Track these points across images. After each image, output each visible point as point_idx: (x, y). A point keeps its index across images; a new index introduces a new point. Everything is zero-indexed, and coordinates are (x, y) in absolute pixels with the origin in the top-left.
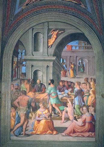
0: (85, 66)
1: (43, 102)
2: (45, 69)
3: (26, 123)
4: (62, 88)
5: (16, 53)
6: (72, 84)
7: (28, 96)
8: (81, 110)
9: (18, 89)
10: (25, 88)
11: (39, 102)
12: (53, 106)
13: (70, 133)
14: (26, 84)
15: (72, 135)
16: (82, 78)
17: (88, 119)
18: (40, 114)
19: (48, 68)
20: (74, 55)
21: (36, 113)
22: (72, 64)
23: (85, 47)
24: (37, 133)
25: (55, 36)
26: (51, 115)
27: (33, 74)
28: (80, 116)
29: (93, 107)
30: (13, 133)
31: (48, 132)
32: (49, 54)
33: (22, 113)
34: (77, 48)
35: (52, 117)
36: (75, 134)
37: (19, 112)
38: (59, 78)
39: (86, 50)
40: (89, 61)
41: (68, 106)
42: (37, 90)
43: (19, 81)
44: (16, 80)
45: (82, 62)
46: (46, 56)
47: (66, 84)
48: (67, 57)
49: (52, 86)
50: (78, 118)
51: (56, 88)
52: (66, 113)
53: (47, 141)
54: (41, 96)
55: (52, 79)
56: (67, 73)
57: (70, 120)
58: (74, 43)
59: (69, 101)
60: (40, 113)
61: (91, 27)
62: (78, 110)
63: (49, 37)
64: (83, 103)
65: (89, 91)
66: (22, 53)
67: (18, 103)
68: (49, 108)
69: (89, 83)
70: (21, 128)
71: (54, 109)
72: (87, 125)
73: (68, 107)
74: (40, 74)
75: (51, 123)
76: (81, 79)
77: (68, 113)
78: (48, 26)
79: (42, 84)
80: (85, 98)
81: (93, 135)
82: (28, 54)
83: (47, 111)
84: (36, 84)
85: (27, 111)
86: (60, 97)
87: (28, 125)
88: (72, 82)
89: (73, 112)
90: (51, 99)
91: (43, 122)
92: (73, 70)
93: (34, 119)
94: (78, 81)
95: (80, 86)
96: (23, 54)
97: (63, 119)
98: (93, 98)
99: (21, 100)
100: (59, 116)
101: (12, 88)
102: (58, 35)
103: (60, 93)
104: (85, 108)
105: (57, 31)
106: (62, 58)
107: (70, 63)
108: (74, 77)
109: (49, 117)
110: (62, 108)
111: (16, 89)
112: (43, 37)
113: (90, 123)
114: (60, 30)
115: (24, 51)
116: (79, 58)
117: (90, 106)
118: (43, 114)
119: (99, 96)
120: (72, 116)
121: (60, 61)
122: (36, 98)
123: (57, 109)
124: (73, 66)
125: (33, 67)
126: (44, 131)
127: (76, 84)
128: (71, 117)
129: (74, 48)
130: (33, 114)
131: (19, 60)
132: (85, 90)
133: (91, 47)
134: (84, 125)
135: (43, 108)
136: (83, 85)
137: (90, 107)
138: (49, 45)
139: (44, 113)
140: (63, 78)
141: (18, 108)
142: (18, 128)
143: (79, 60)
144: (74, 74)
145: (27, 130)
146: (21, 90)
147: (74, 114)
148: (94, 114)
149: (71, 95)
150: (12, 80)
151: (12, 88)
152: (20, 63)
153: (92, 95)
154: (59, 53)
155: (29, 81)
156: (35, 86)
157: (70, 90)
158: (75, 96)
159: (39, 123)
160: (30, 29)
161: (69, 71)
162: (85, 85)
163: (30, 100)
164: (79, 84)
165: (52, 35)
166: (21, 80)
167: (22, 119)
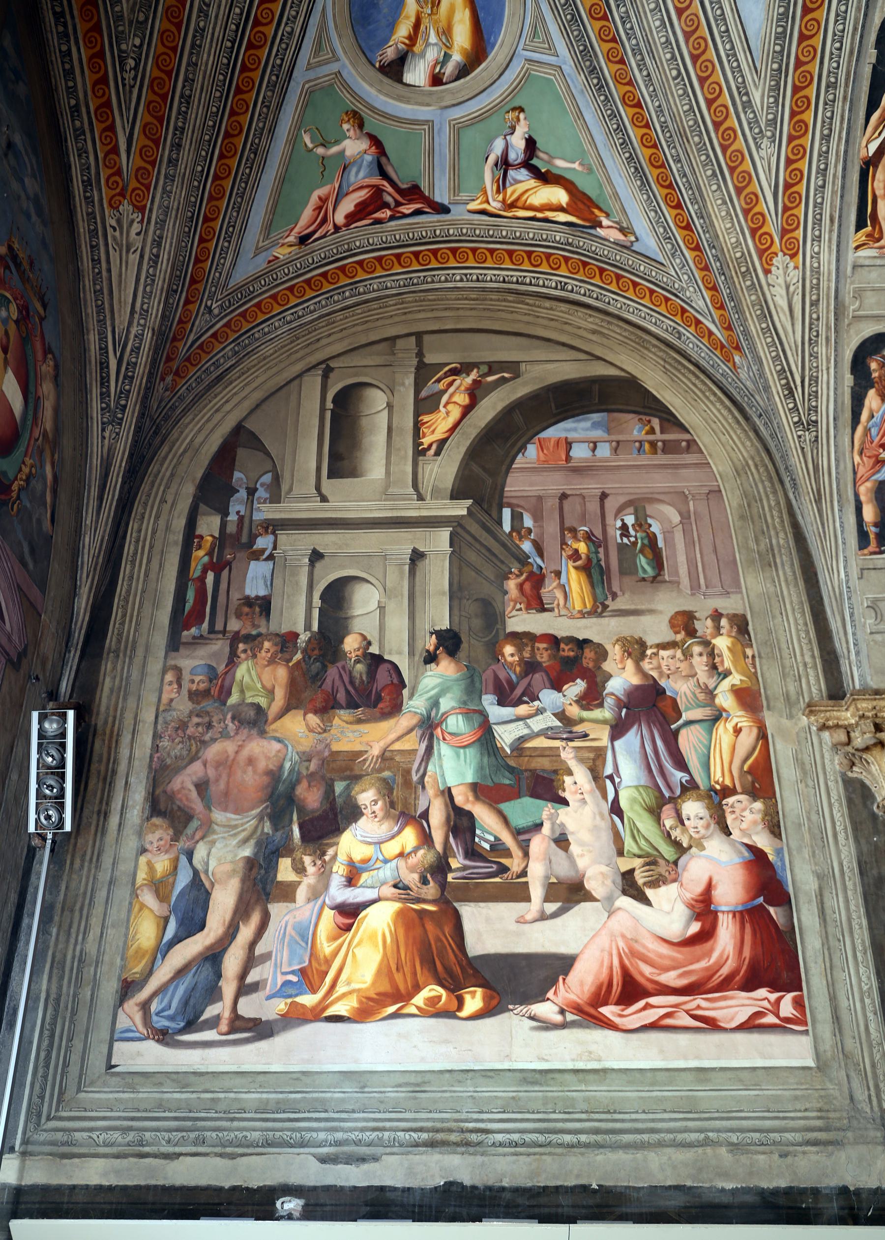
0: (661, 544)
1: (386, 774)
2: (402, 572)
3: (246, 933)
4: (522, 677)
5: (214, 489)
6: (589, 654)
7: (279, 741)
8: (668, 823)
9: (216, 688)
10: (259, 686)
11: (355, 778)
12: (459, 800)
13: (601, 997)
14: (272, 661)
15: (617, 1020)
16: (651, 612)
17: (730, 893)
18: (357, 857)
19: (420, 565)
20: (591, 486)
21: (331, 852)
22: (576, 538)
23: (653, 444)
24: (329, 1012)
25: (462, 399)
26: (440, 868)
27: (317, 602)
28: (662, 869)
29: (754, 794)
30: (138, 1017)
31: (419, 999)
32: (426, 488)
33: (223, 856)
34: (604, 451)
35: (450, 877)
36: (641, 1004)
37: (200, 853)
38: (492, 617)
39: (662, 459)
40: (685, 516)
41: (567, 795)
42: (341, 696)
43: (220, 646)
44: (199, 640)
45: (641, 524)
46: (404, 497)
47: (544, 657)
48: (540, 498)
49: (446, 669)
50: (655, 883)
51: (472, 689)
52: (553, 845)
53: (412, 1079)
54: (370, 738)
55: (445, 624)
56: (550, 589)
57: (588, 897)
58: (581, 433)
59: (573, 764)
60: (359, 852)
61: (677, 342)
62: (646, 825)
63: (426, 405)
64: (679, 776)
65: (711, 694)
66: (251, 492)
67: (202, 787)
68: (425, 815)
69: (706, 643)
70: (207, 971)
71: (461, 824)
72: (727, 934)
73: (565, 802)
74: (365, 602)
75: (439, 926)
76: (645, 620)
77: (574, 848)
78: (420, 355)
79: (376, 661)
80: (689, 741)
81: (787, 1008)
82: (295, 491)
83: (409, 837)
84: (333, 662)
85: (259, 844)
86: (506, 736)
87: (259, 950)
88: (586, 641)
89: (606, 837)
90: (444, 750)
91: (380, 919)
92: (587, 569)
93: (315, 894)
94: (626, 633)
95: (646, 665)
96: (261, 493)
97: (537, 892)
98: (748, 738)
99: (225, 764)
100: (504, 869)
101: (166, 688)
102: (475, 394)
103: (507, 712)
104: (693, 808)
105: (474, 375)
106: (509, 505)
107: (563, 529)
108: (599, 609)
109: (424, 881)
110: (522, 810)
111: (194, 696)
112: (390, 406)
113: (752, 917)
114: (492, 367)
115: (267, 478)
116: (622, 500)
117: (727, 792)
118: (386, 861)
119: (785, 722)
120: (604, 869)
121: (500, 523)
122: (335, 747)
123: (483, 814)
124: (582, 547)
125: (318, 565)
126: (385, 987)
127: (614, 652)
128: (598, 877)
129: (580, 452)
130: (307, 860)
131: (231, 529)
132: (680, 688)
133: (688, 441)
134: (706, 935)
135: (380, 814)
136: (662, 653)
137: (730, 800)
138: (426, 441)
139: (392, 848)
140: (521, 621)
141: (195, 824)
142: (180, 973)
143: (620, 510)
144: (599, 591)
145: (255, 987)
146: (234, 699)
147: (620, 853)
148: (768, 850)
149: (582, 720)
150: (174, 644)
151: (169, 692)
152: (237, 545)
153: (738, 717)
154: (489, 481)
155: (287, 641)
156: (332, 672)
157: (577, 687)
158: (618, 730)
159: (348, 928)
160: (309, 370)
161: (558, 574)
162: (679, 654)
163: (287, 765)
164: (636, 649)
165: (444, 391)
166: (236, 638)
167: (223, 901)
